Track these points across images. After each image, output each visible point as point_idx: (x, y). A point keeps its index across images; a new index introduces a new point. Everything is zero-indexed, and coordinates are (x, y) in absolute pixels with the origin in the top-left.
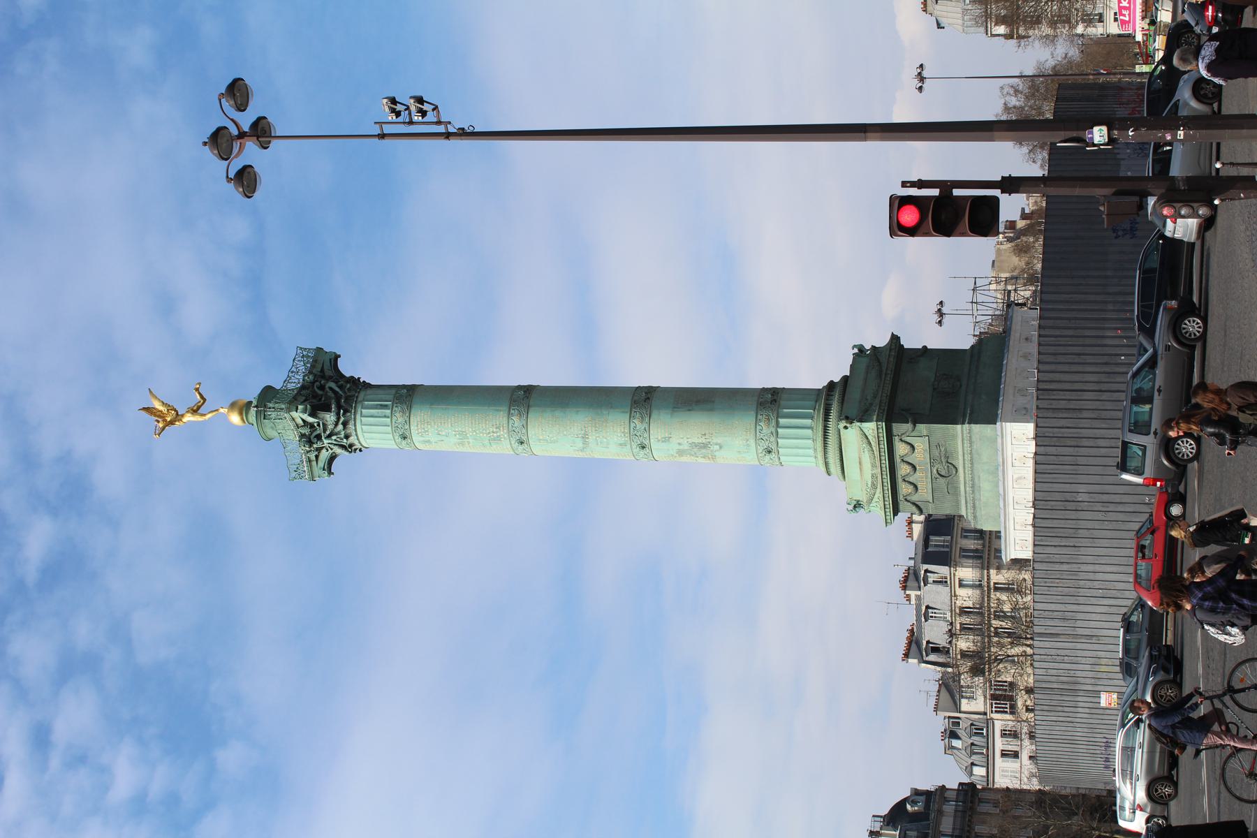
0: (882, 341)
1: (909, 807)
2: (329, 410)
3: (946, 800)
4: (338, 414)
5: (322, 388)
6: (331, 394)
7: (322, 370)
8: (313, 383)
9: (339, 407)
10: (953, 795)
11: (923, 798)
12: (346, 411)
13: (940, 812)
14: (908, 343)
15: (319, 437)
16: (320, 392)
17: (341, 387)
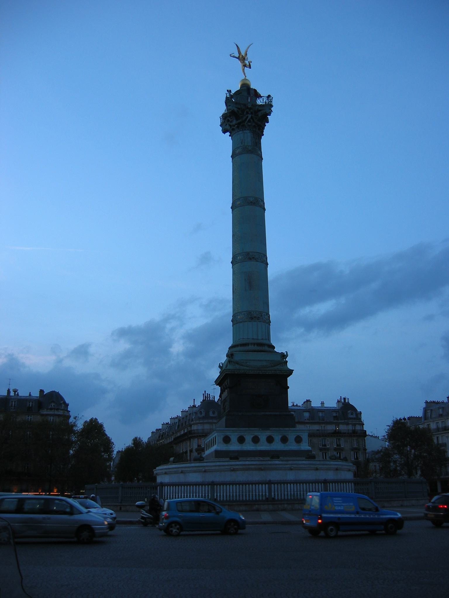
0: (290, 366)
1: (349, 412)
2: (237, 119)
3: (354, 425)
4: (236, 124)
5: (247, 113)
6: (245, 118)
7: (260, 110)
8: (248, 108)
9: (239, 124)
10: (358, 427)
11: (354, 416)
12: (238, 127)
13: (348, 424)
14: (290, 380)
15: (228, 121)
16: (245, 113)
17: (249, 121)
